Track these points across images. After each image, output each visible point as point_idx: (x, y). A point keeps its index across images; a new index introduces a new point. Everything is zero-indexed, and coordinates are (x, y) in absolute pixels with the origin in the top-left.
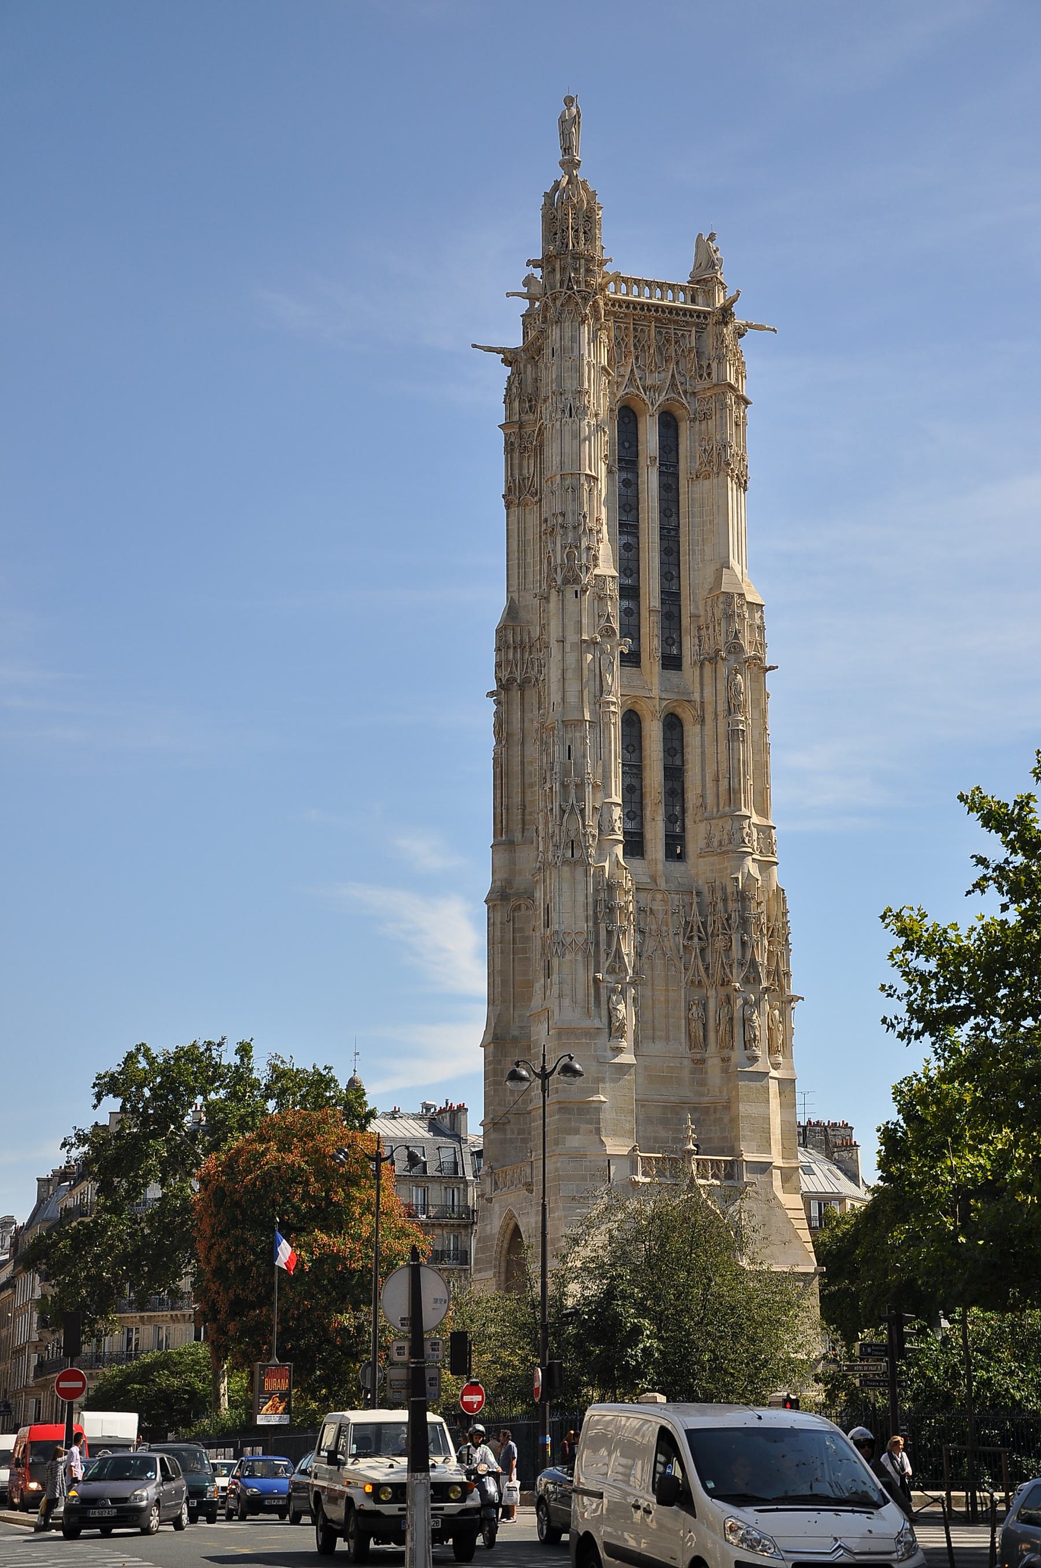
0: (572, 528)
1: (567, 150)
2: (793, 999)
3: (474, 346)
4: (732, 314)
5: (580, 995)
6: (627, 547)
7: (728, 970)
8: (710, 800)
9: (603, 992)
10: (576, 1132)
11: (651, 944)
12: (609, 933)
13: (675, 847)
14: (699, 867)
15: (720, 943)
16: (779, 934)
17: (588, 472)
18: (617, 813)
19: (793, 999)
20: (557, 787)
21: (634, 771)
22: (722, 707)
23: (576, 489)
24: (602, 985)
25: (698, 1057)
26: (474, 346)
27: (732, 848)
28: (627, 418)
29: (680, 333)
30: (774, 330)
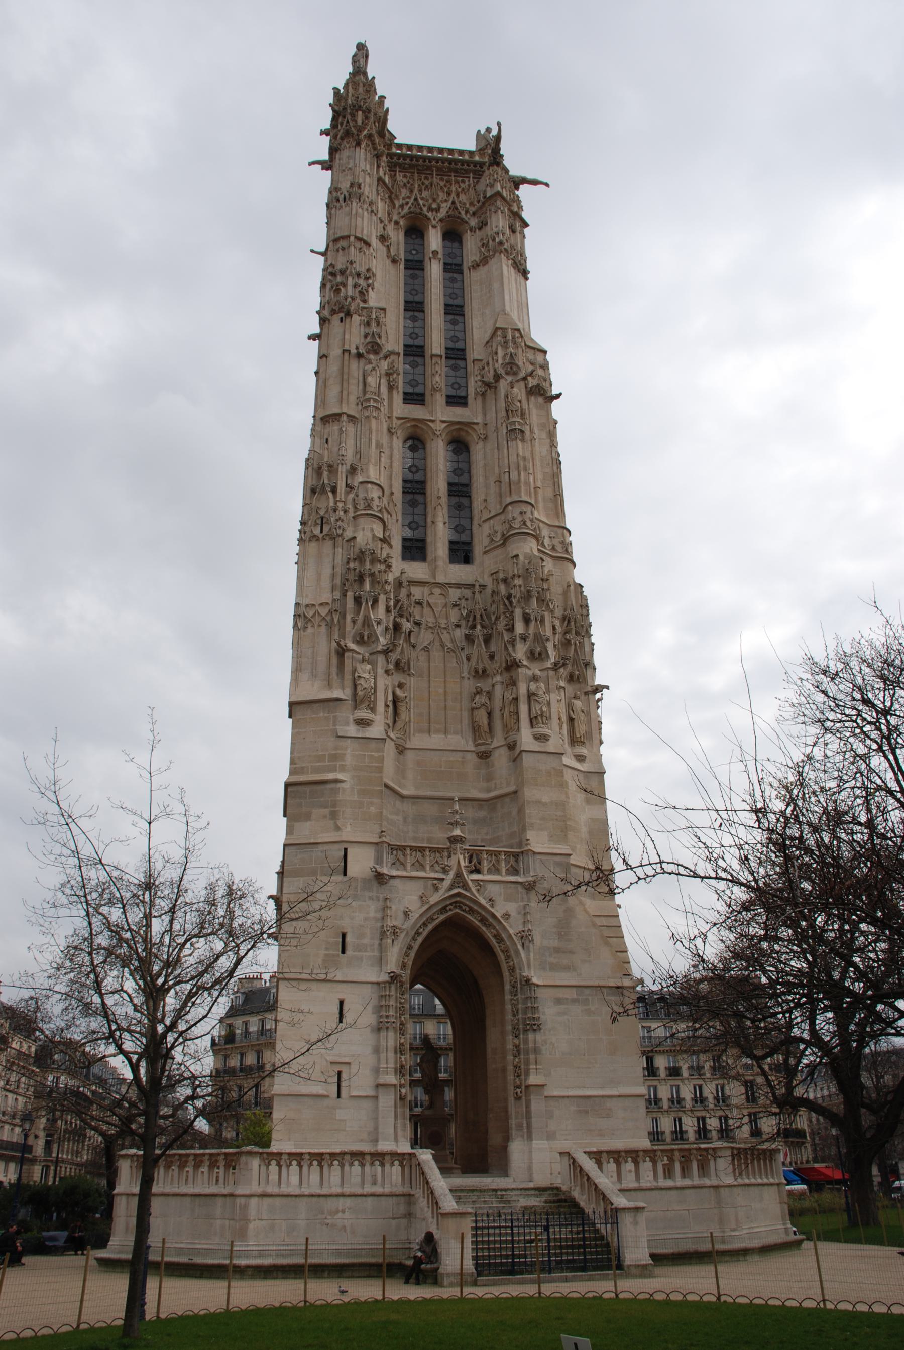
2: (598, 689)
3: (312, 251)
4: (502, 156)
5: (322, 667)
7: (510, 649)
9: (347, 662)
12: (358, 600)
15: (501, 625)
17: (360, 236)
19: (598, 689)
24: (346, 654)
25: (483, 748)
26: (312, 251)
29: (460, 179)
30: (547, 185)
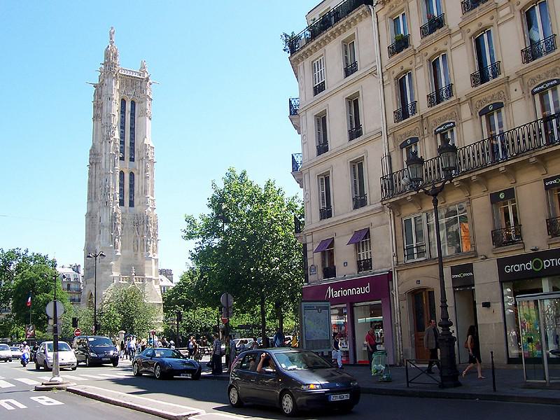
0: (109, 126)
1: (111, 39)
6: (122, 132)
8: (140, 193)
10: (106, 271)
11: (125, 226)
13: (132, 204)
14: (137, 208)
15: (141, 227)
16: (156, 225)
18: (118, 195)
20: (103, 189)
21: (122, 185)
22: (144, 171)
23: (110, 117)
27: (145, 204)
28: (123, 102)
